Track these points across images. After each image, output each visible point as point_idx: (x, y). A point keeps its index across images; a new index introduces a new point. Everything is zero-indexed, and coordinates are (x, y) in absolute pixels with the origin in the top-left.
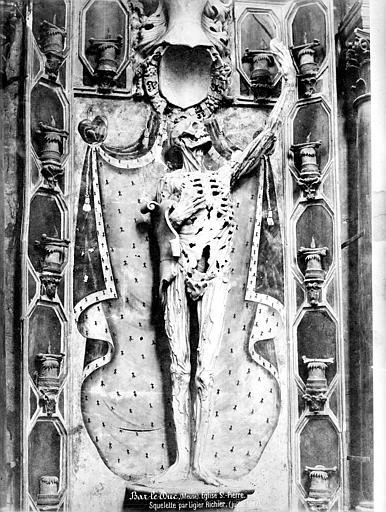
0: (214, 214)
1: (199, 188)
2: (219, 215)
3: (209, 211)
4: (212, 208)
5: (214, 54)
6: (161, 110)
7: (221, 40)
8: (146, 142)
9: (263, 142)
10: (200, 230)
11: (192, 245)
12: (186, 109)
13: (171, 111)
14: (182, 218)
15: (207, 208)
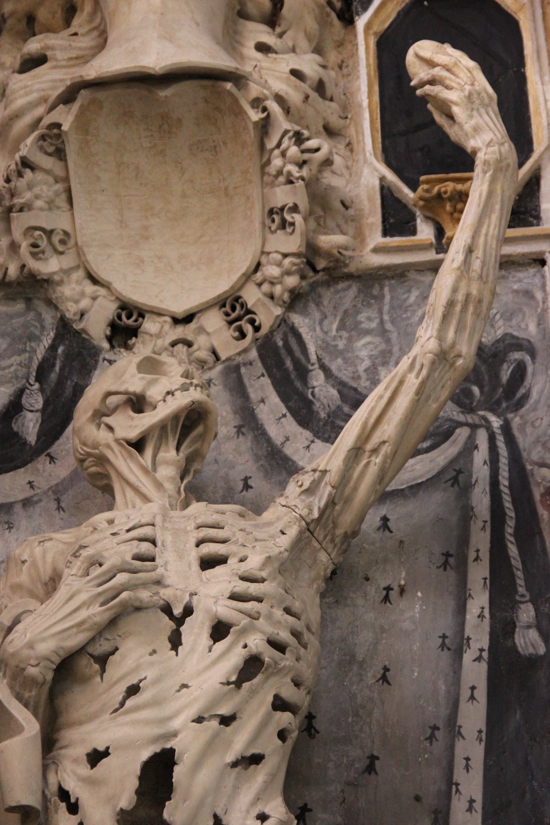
0: (195, 632)
1: (145, 547)
2: (219, 630)
3: (180, 621)
4: (188, 611)
5: (257, 103)
6: (96, 327)
7: (296, 73)
8: (30, 425)
9: (413, 382)
10: (133, 690)
11: (96, 757)
12: (188, 319)
13: (134, 332)
14: (45, 648)
15: (167, 609)
